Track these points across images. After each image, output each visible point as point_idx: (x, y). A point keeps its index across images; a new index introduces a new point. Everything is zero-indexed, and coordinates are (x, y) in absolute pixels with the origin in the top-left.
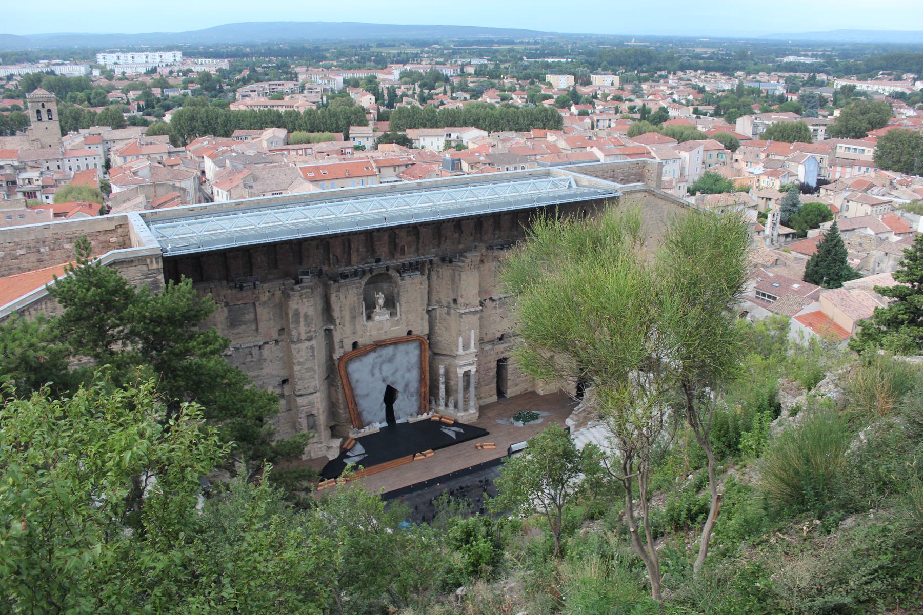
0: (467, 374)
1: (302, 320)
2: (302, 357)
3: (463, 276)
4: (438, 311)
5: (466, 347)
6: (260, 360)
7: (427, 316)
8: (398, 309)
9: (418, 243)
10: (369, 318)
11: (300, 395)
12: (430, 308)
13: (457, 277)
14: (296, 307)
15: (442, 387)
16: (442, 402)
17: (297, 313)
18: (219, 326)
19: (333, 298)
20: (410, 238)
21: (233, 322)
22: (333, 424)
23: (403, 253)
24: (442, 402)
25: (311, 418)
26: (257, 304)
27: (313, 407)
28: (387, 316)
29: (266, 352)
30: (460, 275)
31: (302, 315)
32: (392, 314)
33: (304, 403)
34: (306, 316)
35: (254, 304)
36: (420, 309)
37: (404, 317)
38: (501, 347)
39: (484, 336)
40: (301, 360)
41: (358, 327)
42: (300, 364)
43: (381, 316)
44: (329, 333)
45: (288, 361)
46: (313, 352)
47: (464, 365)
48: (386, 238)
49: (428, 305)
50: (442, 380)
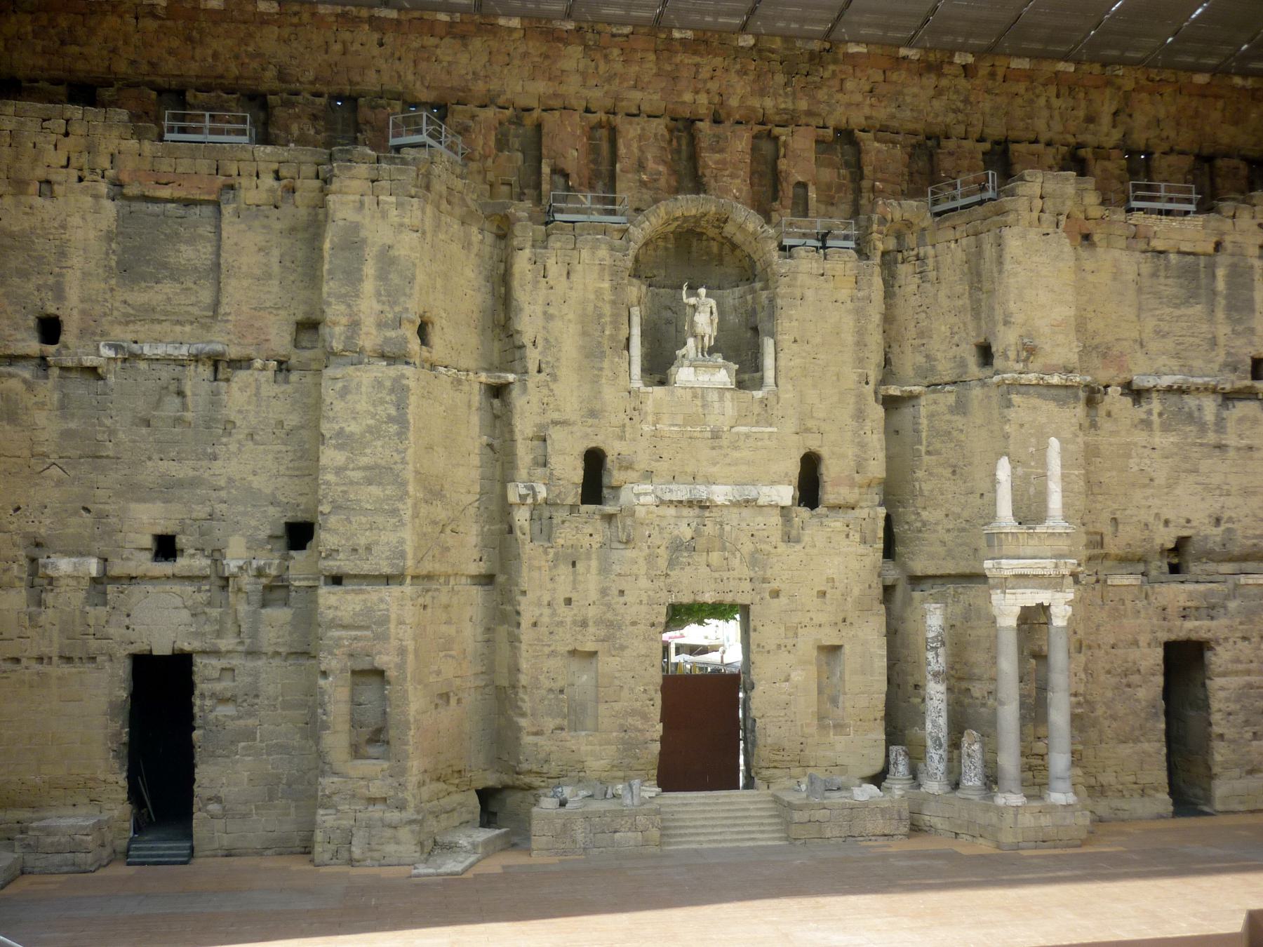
0: (1034, 619)
1: (369, 269)
2: (355, 416)
3: (1014, 243)
4: (925, 407)
5: (1030, 512)
6: (209, 423)
7: (880, 410)
8: (769, 362)
9: (858, 191)
10: (658, 368)
11: (337, 580)
12: (894, 390)
13: (989, 251)
14: (352, 216)
15: (936, 694)
16: (936, 760)
17: (353, 244)
18: (76, 260)
19: (522, 263)
20: (827, 175)
21: (133, 262)
22: (491, 780)
23: (801, 207)
24: (936, 760)
25: (369, 694)
26: (227, 210)
27: (384, 637)
28: (722, 376)
29: (239, 393)
31: (371, 253)
33: (345, 614)
34: (387, 260)
35: (217, 204)
36: (851, 376)
37: (788, 394)
38: (1176, 593)
39: (1107, 529)
40: (353, 428)
41: (611, 396)
42: (345, 441)
43: (701, 376)
45: (305, 443)
46: (401, 406)
47: (1022, 579)
48: (741, 143)
49: (883, 382)
50: (936, 661)
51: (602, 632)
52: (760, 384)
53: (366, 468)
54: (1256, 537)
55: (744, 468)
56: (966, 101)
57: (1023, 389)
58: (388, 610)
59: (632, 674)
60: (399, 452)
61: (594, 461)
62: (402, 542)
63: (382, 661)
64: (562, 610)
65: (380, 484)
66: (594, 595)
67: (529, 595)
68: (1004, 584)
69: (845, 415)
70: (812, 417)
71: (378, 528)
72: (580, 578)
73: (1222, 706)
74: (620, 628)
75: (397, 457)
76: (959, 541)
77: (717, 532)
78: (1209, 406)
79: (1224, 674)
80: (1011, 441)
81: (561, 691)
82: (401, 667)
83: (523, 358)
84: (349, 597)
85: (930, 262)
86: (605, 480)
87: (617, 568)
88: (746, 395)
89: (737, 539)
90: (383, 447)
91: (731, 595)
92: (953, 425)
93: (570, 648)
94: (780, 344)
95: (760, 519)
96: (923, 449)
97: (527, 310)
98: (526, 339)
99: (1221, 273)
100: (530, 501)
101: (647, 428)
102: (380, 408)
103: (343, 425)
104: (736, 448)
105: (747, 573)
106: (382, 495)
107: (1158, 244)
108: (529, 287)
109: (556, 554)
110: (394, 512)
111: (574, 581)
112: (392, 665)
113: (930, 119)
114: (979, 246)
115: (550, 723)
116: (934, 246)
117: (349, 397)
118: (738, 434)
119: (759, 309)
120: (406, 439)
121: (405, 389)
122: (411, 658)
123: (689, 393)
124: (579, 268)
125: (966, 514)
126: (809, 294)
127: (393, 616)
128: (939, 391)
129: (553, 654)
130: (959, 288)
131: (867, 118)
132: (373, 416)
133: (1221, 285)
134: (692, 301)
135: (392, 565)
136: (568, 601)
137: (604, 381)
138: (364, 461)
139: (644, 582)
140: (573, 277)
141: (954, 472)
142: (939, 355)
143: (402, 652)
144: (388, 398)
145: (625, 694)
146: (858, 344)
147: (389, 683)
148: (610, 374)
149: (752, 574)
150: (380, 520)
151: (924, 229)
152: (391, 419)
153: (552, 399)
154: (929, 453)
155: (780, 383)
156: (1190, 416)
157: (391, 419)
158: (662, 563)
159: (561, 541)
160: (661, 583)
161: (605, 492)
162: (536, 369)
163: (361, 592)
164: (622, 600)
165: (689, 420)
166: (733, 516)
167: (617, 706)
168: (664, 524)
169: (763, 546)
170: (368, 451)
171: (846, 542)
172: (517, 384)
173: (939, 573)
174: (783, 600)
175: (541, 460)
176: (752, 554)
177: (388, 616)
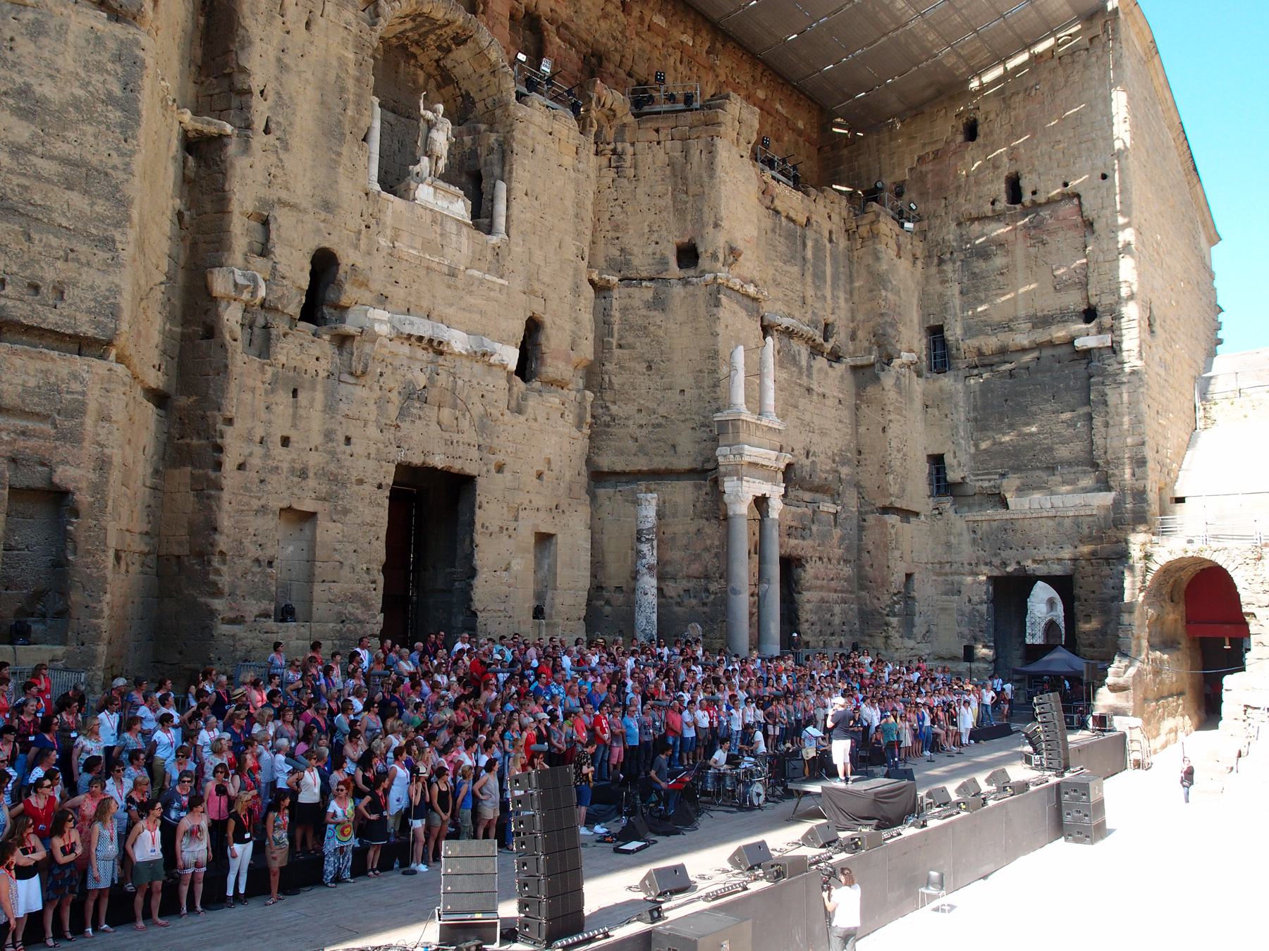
4: (618, 297)
8: (501, 207)
10: (395, 179)
27: (74, 438)
30: (711, 152)
32: (482, 216)
37: (517, 250)
40: (46, 89)
41: (347, 192)
44: (203, 157)
51: (324, 489)
52: (489, 230)
53: (65, 161)
54: (827, 472)
55: (477, 317)
56: (622, 33)
57: (729, 292)
58: (84, 394)
59: (353, 547)
60: (122, 154)
61: (324, 265)
62: (115, 291)
63: (66, 475)
64: (278, 450)
65: (86, 192)
66: (317, 439)
67: (238, 423)
68: (737, 472)
69: (567, 284)
70: (538, 280)
71: (78, 261)
72: (302, 412)
73: (809, 616)
74: (344, 485)
75: (116, 160)
76: (654, 437)
77: (450, 386)
78: (804, 351)
79: (809, 589)
80: (719, 338)
81: (270, 564)
82: (98, 489)
83: (244, 108)
84: (18, 362)
85: (628, 158)
86: (331, 295)
87: (343, 407)
88: (481, 236)
89: (468, 397)
90: (96, 136)
91: (460, 461)
92: (651, 320)
93: (285, 504)
94: (514, 192)
95: (489, 379)
96: (614, 342)
97: (258, 47)
98: (256, 83)
99: (810, 244)
100: (246, 296)
101: (384, 242)
102: (96, 78)
103: (32, 81)
104: (471, 292)
105: (474, 438)
106: (88, 210)
107: (778, 204)
108: (262, 19)
109: (275, 375)
110: (107, 243)
111: (295, 417)
112: (84, 485)
113: (597, 36)
114: (686, 152)
115: (252, 607)
116: (633, 144)
117: (44, 41)
118: (472, 276)
119: (482, 151)
120: (134, 137)
121: (138, 63)
122: (115, 475)
123: (428, 218)
124: (321, 21)
125: (662, 410)
126: (539, 148)
127: (92, 406)
128: (635, 286)
129: (263, 510)
130: (660, 189)
131: (552, 10)
132: (85, 85)
133: (809, 254)
134: (429, 115)
135: (97, 325)
136: (285, 441)
137: (341, 170)
138: (61, 148)
139: (373, 431)
140: (314, 28)
141: (649, 368)
142: (636, 250)
143: (103, 464)
144: (110, 66)
145: (346, 572)
146: (577, 216)
147: (76, 514)
148: (349, 164)
149: (481, 442)
150: (83, 249)
151: (624, 125)
152: (110, 99)
153: (279, 172)
154: (620, 346)
155: (513, 232)
156: (794, 357)
157: (110, 99)
158: (393, 411)
159: (282, 359)
160: (390, 434)
161: (326, 310)
162: (263, 127)
163: (42, 357)
164: (348, 449)
165: (427, 245)
166: (467, 370)
167: (336, 588)
168: (397, 363)
169: (493, 411)
170: (72, 135)
171: (561, 422)
172: (234, 138)
173: (628, 470)
174: (507, 474)
175: (257, 247)
176: (481, 418)
177: (84, 404)
